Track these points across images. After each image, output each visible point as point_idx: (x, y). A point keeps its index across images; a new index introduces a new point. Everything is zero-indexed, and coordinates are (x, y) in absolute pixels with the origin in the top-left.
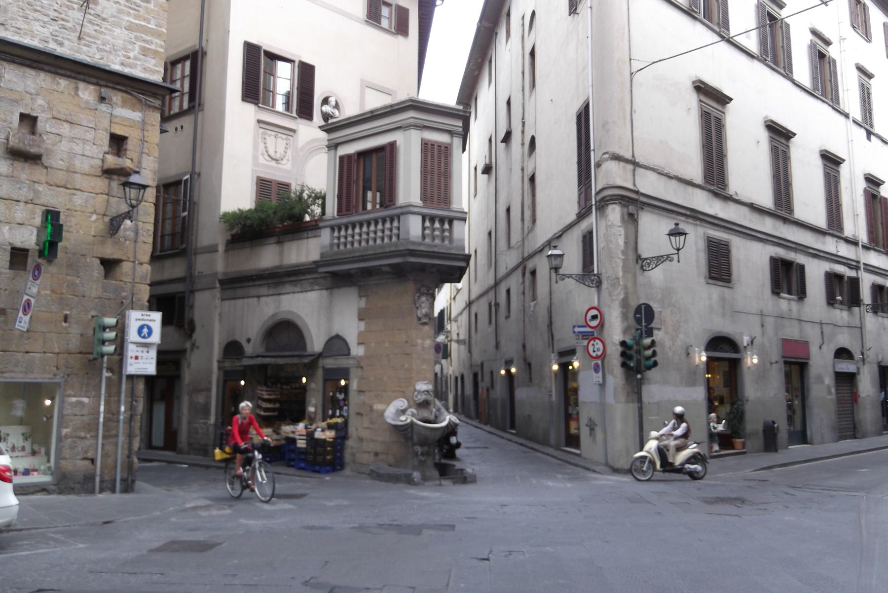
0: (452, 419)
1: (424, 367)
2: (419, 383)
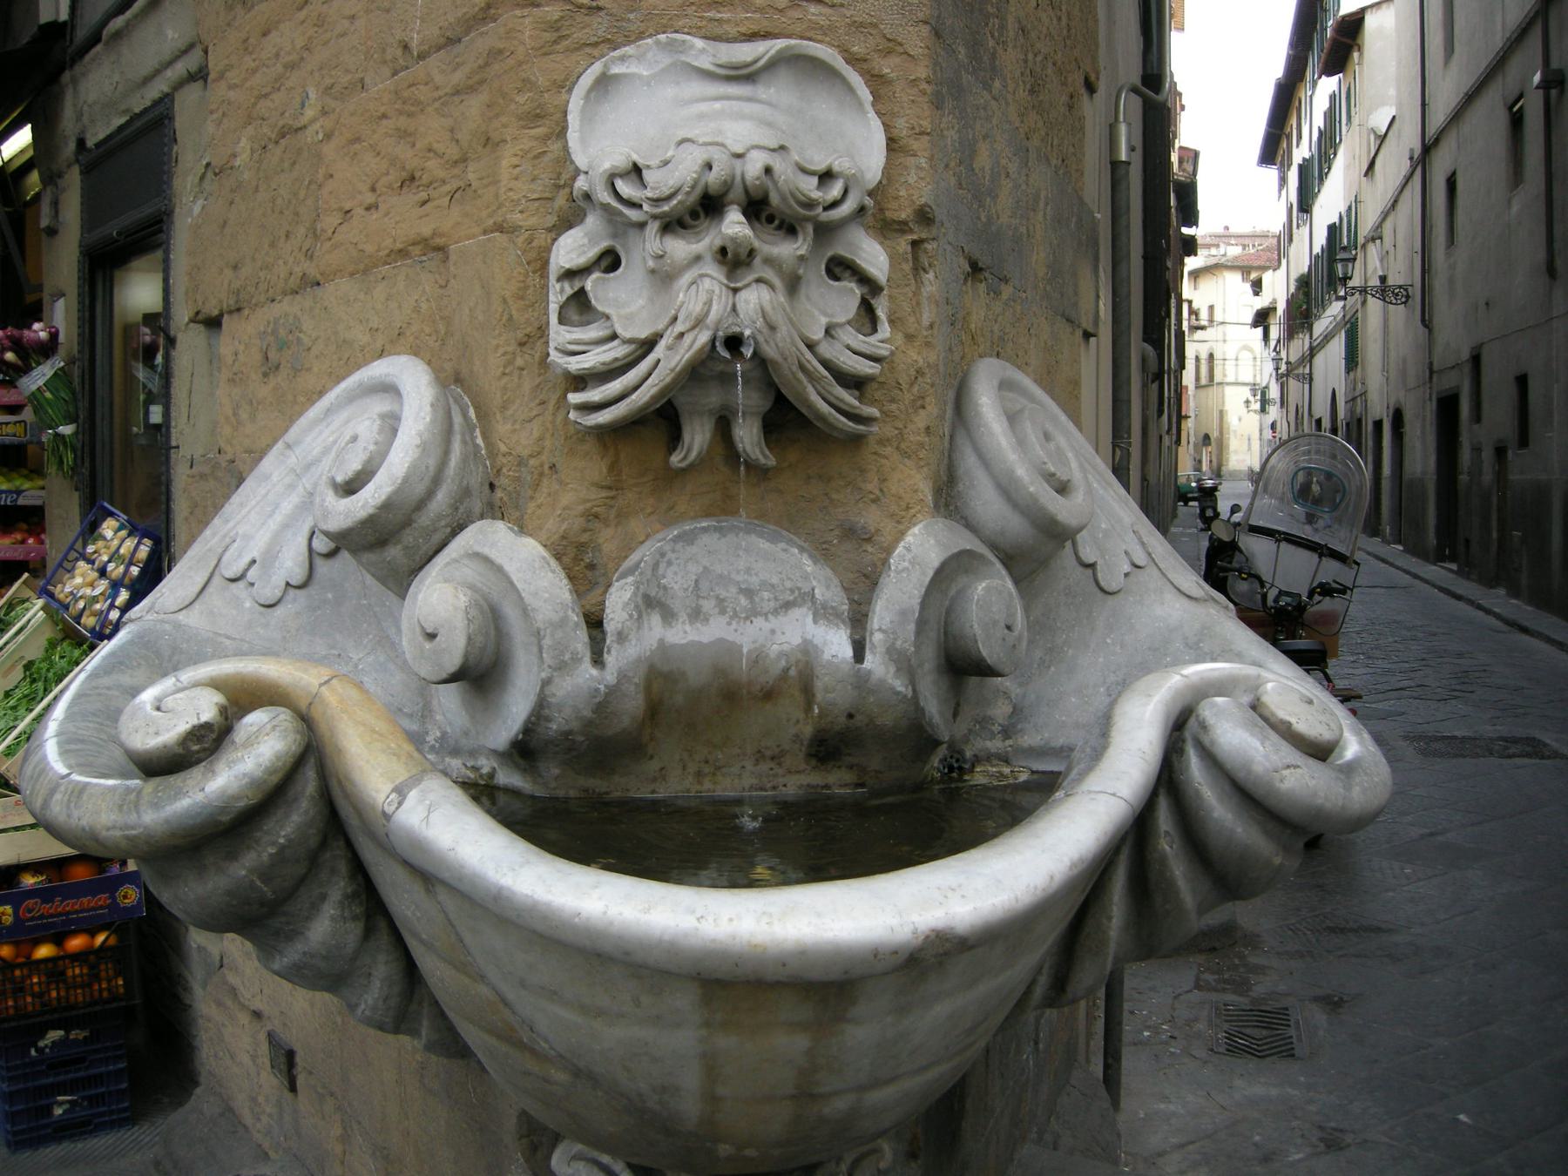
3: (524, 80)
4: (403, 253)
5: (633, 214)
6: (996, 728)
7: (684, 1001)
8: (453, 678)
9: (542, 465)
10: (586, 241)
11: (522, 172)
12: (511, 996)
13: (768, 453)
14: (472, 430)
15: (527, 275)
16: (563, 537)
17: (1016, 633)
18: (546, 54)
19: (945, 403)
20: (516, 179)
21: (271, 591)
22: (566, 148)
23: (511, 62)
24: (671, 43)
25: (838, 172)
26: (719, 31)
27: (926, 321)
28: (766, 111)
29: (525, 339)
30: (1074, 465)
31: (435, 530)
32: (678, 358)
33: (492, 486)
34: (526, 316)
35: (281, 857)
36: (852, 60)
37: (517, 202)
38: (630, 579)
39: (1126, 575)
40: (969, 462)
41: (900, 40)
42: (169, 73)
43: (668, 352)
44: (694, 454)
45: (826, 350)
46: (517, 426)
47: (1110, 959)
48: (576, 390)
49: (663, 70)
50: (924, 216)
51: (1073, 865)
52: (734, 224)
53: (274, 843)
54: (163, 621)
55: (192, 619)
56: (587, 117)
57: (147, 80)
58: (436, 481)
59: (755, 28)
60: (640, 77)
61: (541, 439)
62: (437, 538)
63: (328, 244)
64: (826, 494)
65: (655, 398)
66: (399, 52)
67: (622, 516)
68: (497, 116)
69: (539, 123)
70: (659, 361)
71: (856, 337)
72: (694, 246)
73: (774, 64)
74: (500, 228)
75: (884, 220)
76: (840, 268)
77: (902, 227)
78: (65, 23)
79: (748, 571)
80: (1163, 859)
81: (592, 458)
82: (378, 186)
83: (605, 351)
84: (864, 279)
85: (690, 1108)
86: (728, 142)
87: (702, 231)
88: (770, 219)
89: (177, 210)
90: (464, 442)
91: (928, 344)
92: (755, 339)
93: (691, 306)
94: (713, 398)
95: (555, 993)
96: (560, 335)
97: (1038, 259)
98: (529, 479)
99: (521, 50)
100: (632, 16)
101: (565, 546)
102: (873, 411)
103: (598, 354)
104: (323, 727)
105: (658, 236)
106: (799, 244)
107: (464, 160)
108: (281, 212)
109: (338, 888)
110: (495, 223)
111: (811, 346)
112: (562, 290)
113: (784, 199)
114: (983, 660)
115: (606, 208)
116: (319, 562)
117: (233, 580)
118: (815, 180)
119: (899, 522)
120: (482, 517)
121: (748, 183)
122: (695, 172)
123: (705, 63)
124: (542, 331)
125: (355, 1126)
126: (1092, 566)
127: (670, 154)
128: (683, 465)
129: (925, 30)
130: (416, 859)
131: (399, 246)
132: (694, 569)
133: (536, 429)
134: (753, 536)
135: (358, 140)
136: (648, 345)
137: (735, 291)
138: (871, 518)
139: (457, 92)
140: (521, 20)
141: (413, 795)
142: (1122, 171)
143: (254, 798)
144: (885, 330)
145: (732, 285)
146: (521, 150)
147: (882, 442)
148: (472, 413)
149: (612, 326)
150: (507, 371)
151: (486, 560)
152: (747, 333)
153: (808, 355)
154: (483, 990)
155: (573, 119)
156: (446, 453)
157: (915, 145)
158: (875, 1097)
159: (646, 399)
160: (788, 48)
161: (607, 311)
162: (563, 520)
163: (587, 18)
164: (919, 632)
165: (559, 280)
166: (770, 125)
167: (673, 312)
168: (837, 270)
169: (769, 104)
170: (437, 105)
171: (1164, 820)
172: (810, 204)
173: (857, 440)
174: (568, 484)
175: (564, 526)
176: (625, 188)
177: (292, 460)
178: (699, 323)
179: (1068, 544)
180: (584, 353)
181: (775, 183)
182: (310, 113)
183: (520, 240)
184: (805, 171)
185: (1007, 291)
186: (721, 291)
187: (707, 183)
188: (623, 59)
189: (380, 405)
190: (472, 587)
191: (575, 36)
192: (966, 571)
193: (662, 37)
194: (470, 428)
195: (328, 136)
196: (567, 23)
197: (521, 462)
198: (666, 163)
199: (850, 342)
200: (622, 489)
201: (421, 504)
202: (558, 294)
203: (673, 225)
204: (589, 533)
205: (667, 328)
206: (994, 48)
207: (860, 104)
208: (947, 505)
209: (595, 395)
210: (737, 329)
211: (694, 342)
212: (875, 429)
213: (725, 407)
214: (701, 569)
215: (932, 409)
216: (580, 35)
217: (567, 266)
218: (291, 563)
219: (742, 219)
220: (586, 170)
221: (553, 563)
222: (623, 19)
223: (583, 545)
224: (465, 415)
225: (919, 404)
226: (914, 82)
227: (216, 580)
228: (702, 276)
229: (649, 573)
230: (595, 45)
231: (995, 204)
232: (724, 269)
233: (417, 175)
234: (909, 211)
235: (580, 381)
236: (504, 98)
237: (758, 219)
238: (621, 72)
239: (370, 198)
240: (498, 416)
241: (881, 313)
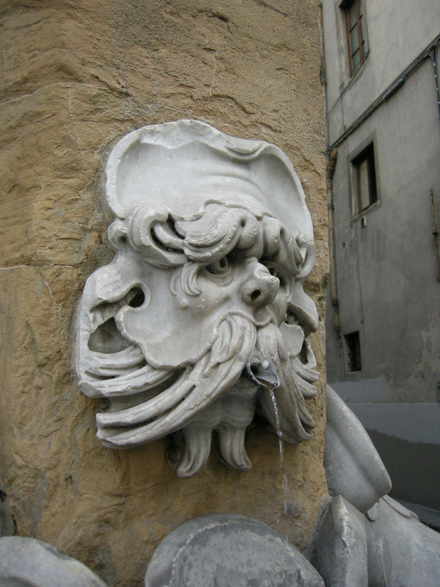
3: (64, 137)
5: (172, 258)
9: (57, 477)
10: (119, 277)
11: (54, 214)
13: (248, 459)
15: (51, 305)
16: (79, 544)
18: (83, 120)
20: (48, 219)
23: (50, 122)
25: (303, 243)
29: (45, 361)
32: (215, 385)
34: (48, 340)
37: (48, 240)
41: (312, 162)
43: (204, 380)
46: (35, 441)
49: (183, 147)
56: (122, 175)
60: (165, 149)
61: (58, 453)
64: (274, 486)
67: (129, 519)
68: (31, 166)
69: (73, 175)
70: (194, 386)
71: (302, 366)
72: (224, 289)
74: (28, 261)
79: (249, 563)
81: (107, 470)
83: (135, 377)
87: (227, 276)
93: (227, 340)
98: (45, 489)
99: (63, 112)
100: (149, 106)
101: (80, 551)
103: (129, 379)
105: (195, 277)
106: (287, 295)
110: (22, 256)
112: (94, 319)
119: (314, 501)
121: (269, 241)
122: (235, 226)
123: (221, 146)
127: (201, 210)
128: (188, 475)
132: (210, 568)
134: (248, 531)
137: (258, 328)
140: (63, 90)
145: (258, 323)
146: (55, 195)
149: (142, 353)
150: (26, 390)
152: (266, 364)
161: (138, 340)
162: (78, 528)
163: (117, 99)
165: (94, 309)
167: (208, 344)
174: (84, 494)
175: (80, 533)
178: (234, 355)
180: (113, 377)
181: (286, 243)
183: (48, 273)
186: (251, 328)
187: (240, 237)
188: (152, 133)
191: (107, 111)
196: (103, 100)
197: (38, 474)
198: (198, 218)
199: (299, 370)
200: (130, 495)
204: (101, 537)
205: (201, 358)
207: (299, 198)
210: (257, 361)
211: (229, 371)
214: (215, 568)
216: (111, 111)
217: (105, 298)
220: (122, 216)
222: (143, 107)
223: (95, 548)
229: (178, 578)
230: (122, 121)
232: (251, 309)
236: (40, 151)
238: (150, 143)
240: (16, 431)
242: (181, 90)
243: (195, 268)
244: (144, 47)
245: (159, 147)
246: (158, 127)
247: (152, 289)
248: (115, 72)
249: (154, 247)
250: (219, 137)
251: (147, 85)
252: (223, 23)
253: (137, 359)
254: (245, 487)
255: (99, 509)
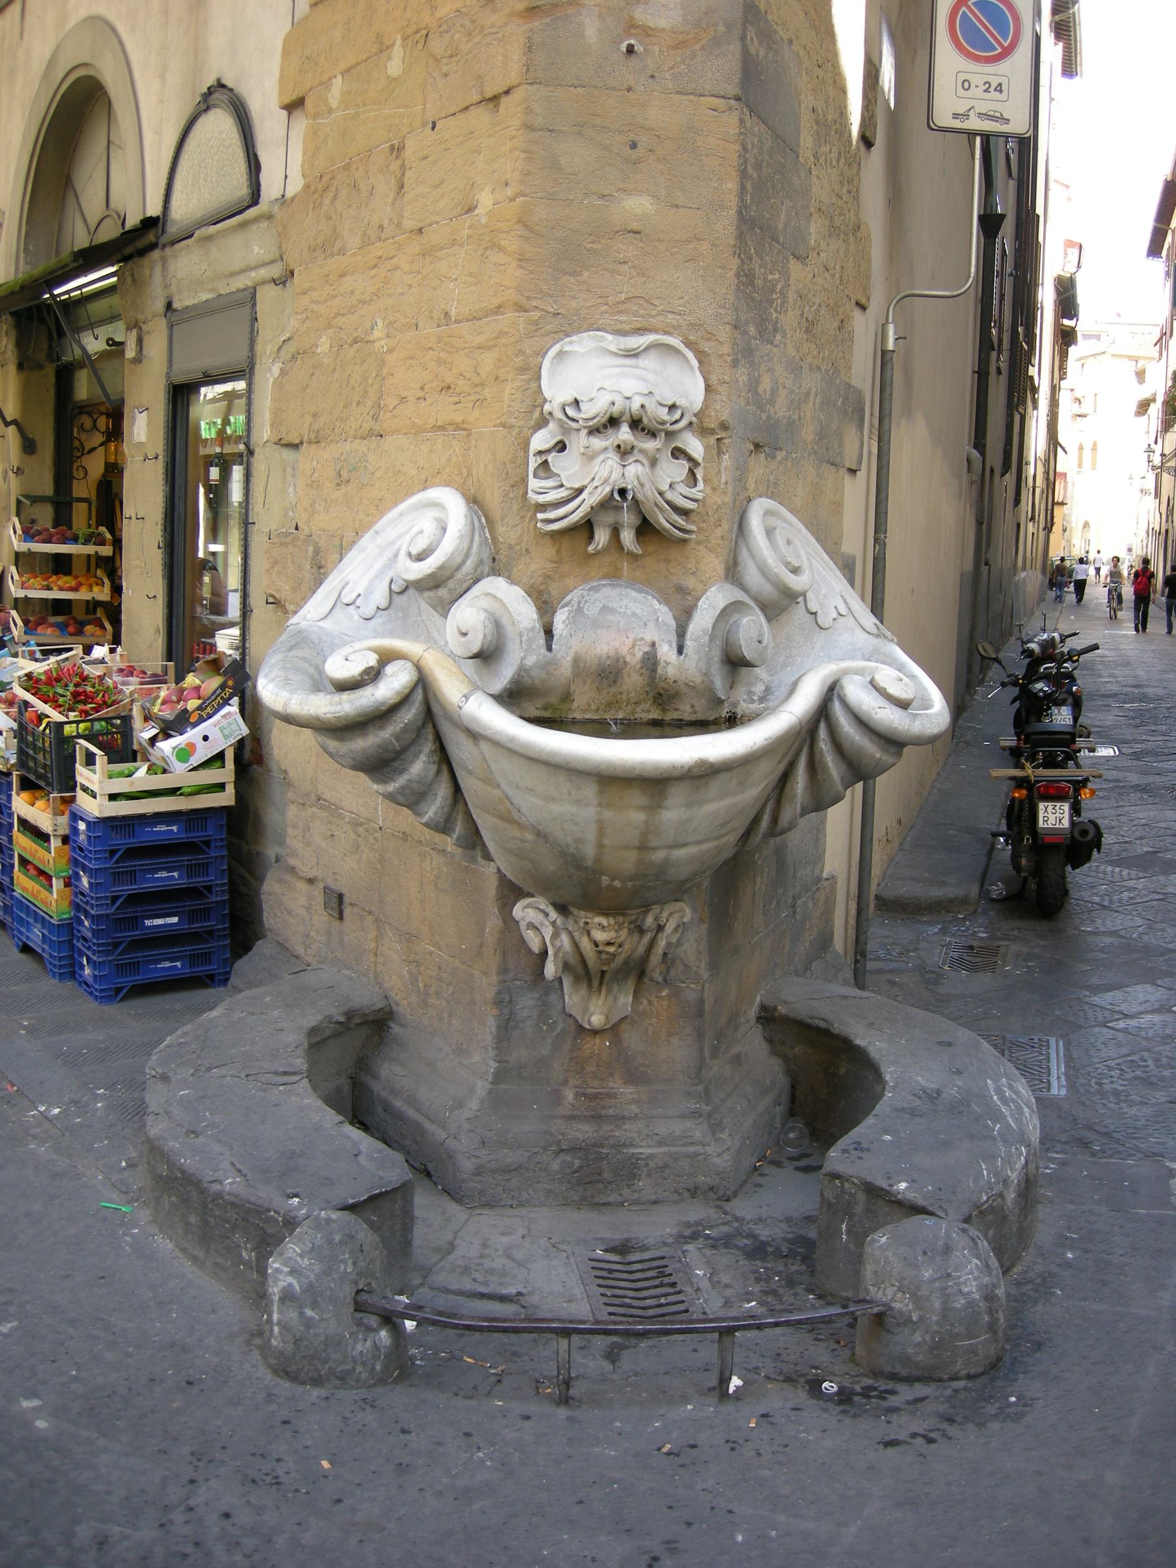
0: (857, 694)
1: (638, 205)
2: (581, 344)
4: (442, 428)
5: (574, 425)
6: (756, 698)
7: (590, 790)
8: (475, 656)
12: (510, 793)
14: (484, 530)
16: (531, 587)
17: (764, 644)
18: (531, 337)
19: (733, 523)
21: (369, 610)
22: (540, 386)
24: (595, 336)
26: (620, 327)
27: (723, 481)
28: (643, 373)
30: (804, 557)
31: (465, 581)
33: (494, 559)
35: (405, 729)
36: (688, 344)
38: (566, 609)
39: (834, 619)
40: (744, 555)
42: (253, 274)
44: (600, 547)
45: (669, 496)
47: (799, 805)
48: (541, 512)
50: (724, 426)
51: (766, 739)
52: (624, 434)
53: (402, 722)
54: (312, 626)
55: (327, 625)
56: (552, 373)
57: (232, 274)
58: (467, 556)
59: (639, 325)
61: (521, 535)
62: (465, 585)
63: (389, 415)
65: (582, 518)
66: (442, 316)
68: (504, 367)
73: (647, 349)
75: (703, 428)
76: (678, 453)
77: (712, 432)
78: (158, 218)
80: (822, 753)
82: (426, 387)
84: (690, 459)
85: (590, 851)
86: (622, 391)
88: (643, 429)
89: (257, 366)
90: (480, 536)
91: (725, 493)
92: (634, 492)
94: (610, 518)
95: (532, 790)
96: (534, 483)
97: (808, 432)
102: (694, 528)
104: (426, 670)
107: (482, 385)
108: (353, 388)
109: (428, 746)
111: (661, 494)
112: (536, 460)
113: (650, 421)
114: (745, 657)
115: (560, 420)
116: (394, 596)
117: (348, 605)
118: (667, 409)
120: (488, 575)
123: (613, 348)
124: (524, 481)
125: (387, 927)
126: (815, 614)
127: (594, 395)
129: (728, 328)
130: (473, 727)
131: (439, 423)
133: (519, 530)
135: (412, 358)
136: (580, 491)
137: (624, 466)
138: (690, 583)
139: (479, 348)
141: (472, 699)
142: (889, 356)
143: (397, 699)
144: (701, 485)
147: (698, 543)
148: (483, 519)
151: (495, 597)
152: (629, 487)
153: (660, 499)
154: (498, 792)
155: (544, 372)
156: (472, 541)
157: (720, 388)
158: (679, 853)
159: (578, 518)
160: (656, 340)
161: (559, 472)
164: (711, 641)
166: (645, 380)
168: (677, 454)
169: (645, 369)
170: (466, 351)
171: (823, 733)
172: (663, 423)
173: (685, 541)
175: (532, 581)
176: (571, 412)
177: (379, 541)
178: (605, 482)
179: (800, 599)
181: (646, 413)
182: (377, 334)
183: (514, 433)
184: (661, 405)
185: (780, 455)
188: (570, 343)
189: (433, 513)
190: (486, 610)
192: (739, 612)
193: (591, 333)
194: (482, 527)
195: (390, 351)
197: (511, 547)
198: (592, 400)
201: (459, 568)
202: (533, 463)
203: (594, 431)
206: (777, 318)
207: (692, 369)
208: (733, 577)
209: (552, 515)
210: (624, 485)
212: (693, 536)
213: (616, 523)
215: (725, 525)
218: (380, 596)
219: (629, 430)
221: (528, 599)
223: (542, 591)
224: (480, 521)
225: (718, 523)
226: (721, 356)
227: (339, 604)
228: (608, 458)
230: (556, 333)
231: (773, 407)
233: (453, 387)
234: (716, 423)
235: (543, 507)
237: (637, 428)
239: (420, 394)
241: (699, 477)
242: (600, 300)
243: (586, 431)
244: (571, 275)
245: (576, 351)
246: (574, 338)
247: (570, 442)
248: (550, 300)
249: (565, 419)
250: (612, 342)
251: (574, 303)
252: (637, 235)
253: (559, 483)
254: (643, 567)
255: (544, 569)
